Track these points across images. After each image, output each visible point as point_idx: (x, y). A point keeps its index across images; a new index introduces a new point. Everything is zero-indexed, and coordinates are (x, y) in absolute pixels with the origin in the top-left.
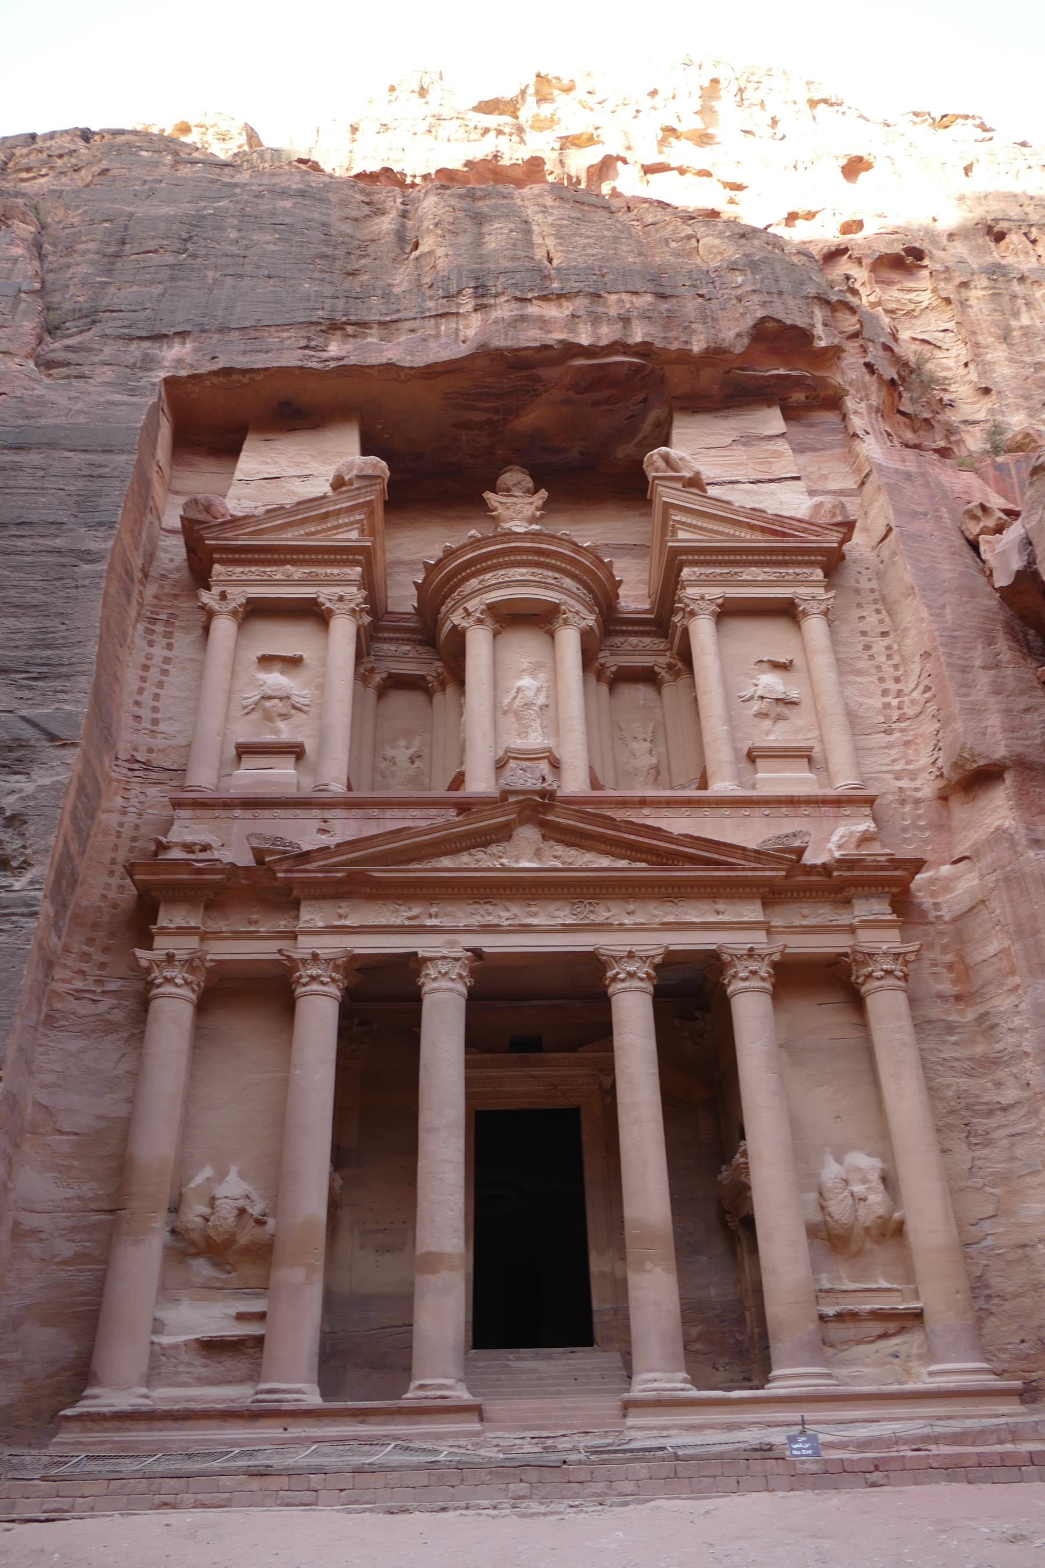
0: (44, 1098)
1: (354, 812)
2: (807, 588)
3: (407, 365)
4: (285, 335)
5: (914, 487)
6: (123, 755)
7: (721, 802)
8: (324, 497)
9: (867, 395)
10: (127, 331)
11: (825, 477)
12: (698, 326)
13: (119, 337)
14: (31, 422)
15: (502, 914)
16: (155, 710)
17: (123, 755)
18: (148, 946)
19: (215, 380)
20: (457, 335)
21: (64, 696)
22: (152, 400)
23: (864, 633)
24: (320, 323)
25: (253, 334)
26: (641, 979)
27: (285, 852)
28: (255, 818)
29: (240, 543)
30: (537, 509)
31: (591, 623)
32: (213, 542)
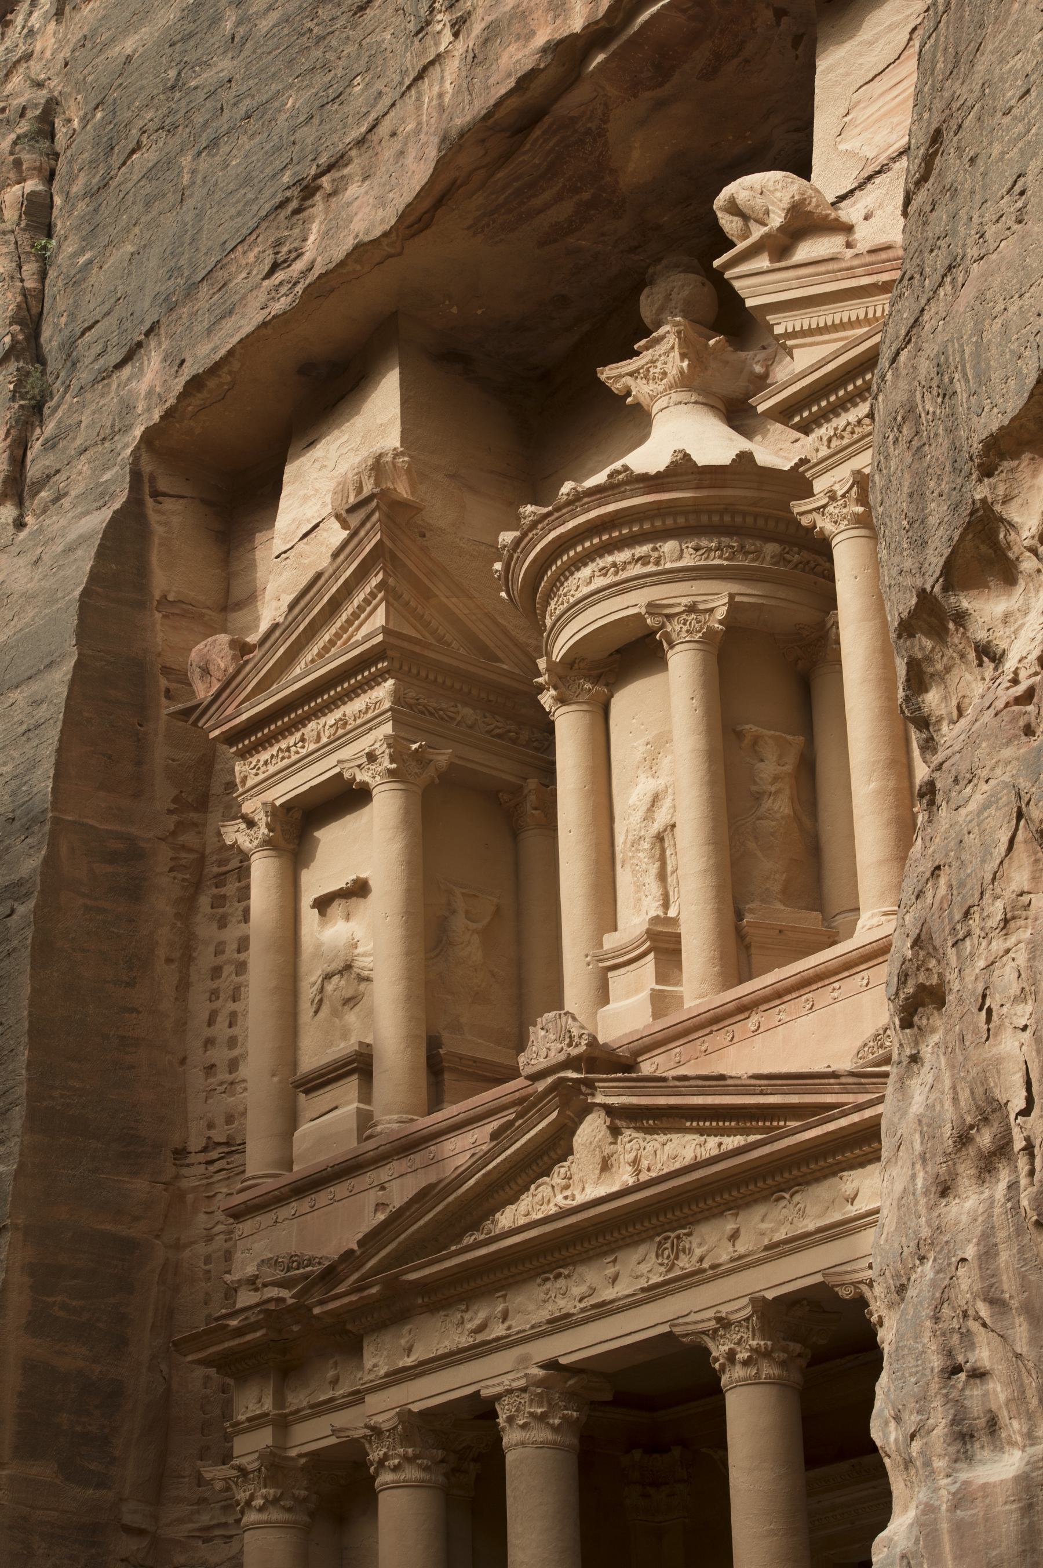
3: (377, 233)
4: (251, 256)
6: (195, 1143)
7: (848, 966)
8: (318, 576)
13: (95, 382)
15: (570, 1292)
18: (226, 1457)
19: (197, 400)
24: (288, 200)
25: (220, 275)
26: (746, 1363)
27: (305, 1277)
28: (313, 1209)
29: (244, 717)
30: (683, 356)
31: (721, 613)
32: (217, 732)
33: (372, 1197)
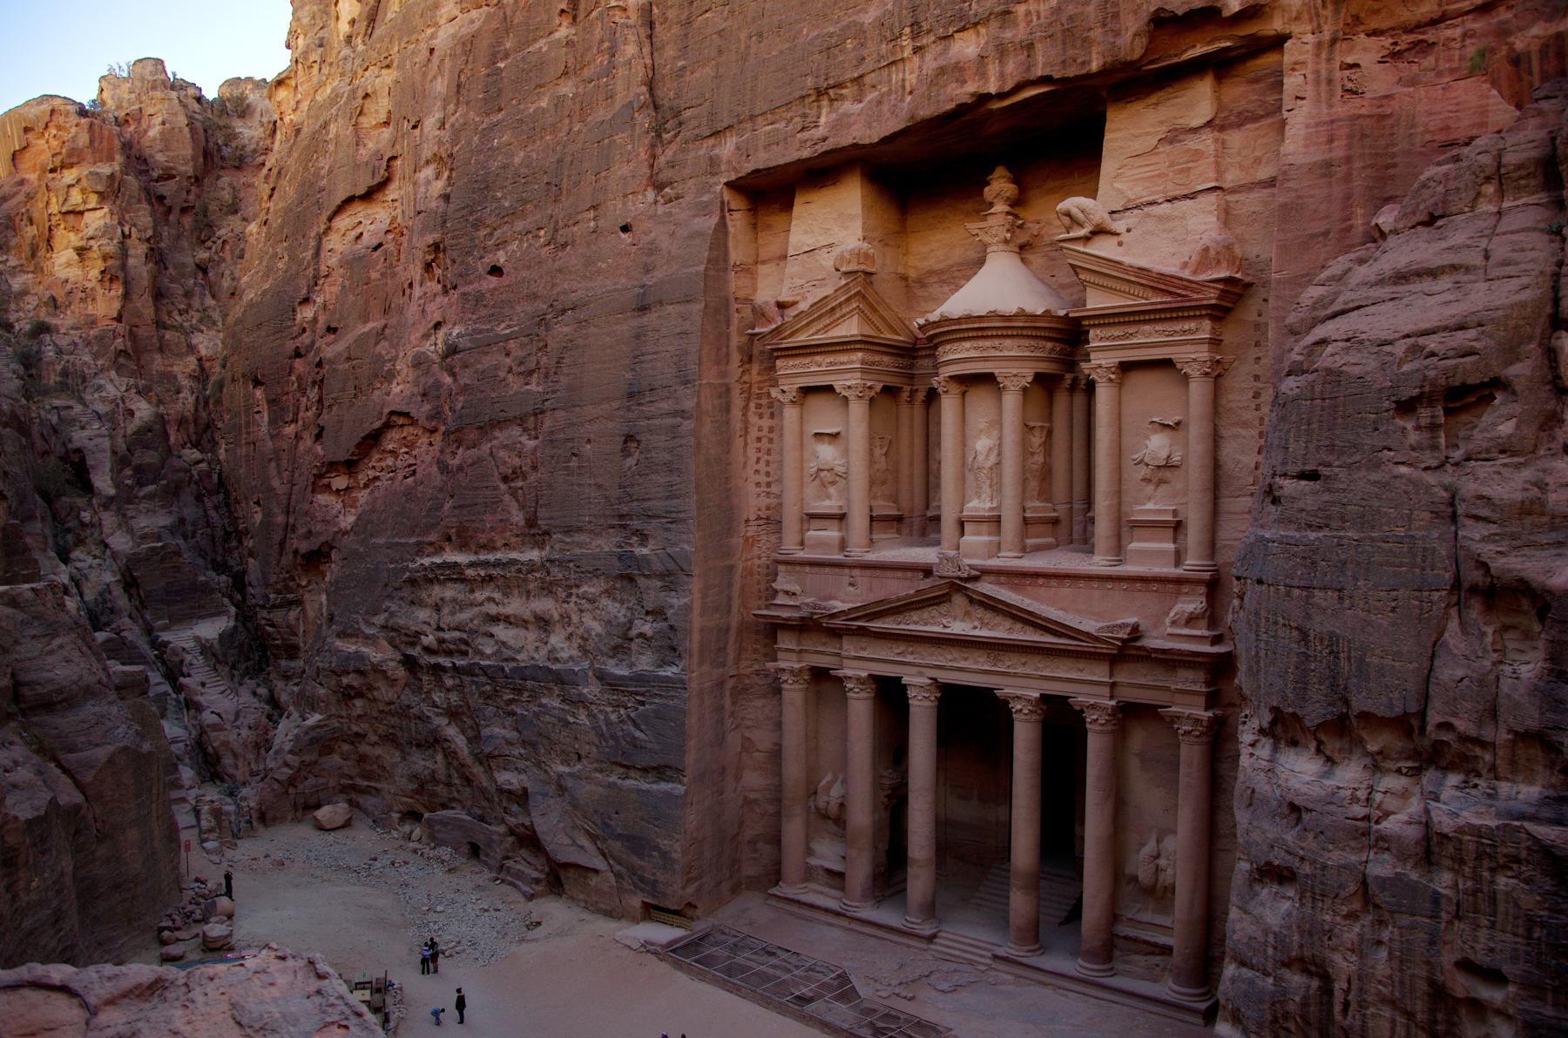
0: (747, 734)
1: (868, 572)
2: (1189, 344)
3: (867, 141)
5: (1330, 185)
6: (752, 517)
9: (1319, 26)
10: (697, 131)
11: (1258, 161)
12: (1097, 33)
14: (649, 280)
16: (768, 474)
17: (752, 517)
20: (904, 87)
21: (685, 537)
22: (714, 220)
23: (1257, 378)
33: (847, 580)
